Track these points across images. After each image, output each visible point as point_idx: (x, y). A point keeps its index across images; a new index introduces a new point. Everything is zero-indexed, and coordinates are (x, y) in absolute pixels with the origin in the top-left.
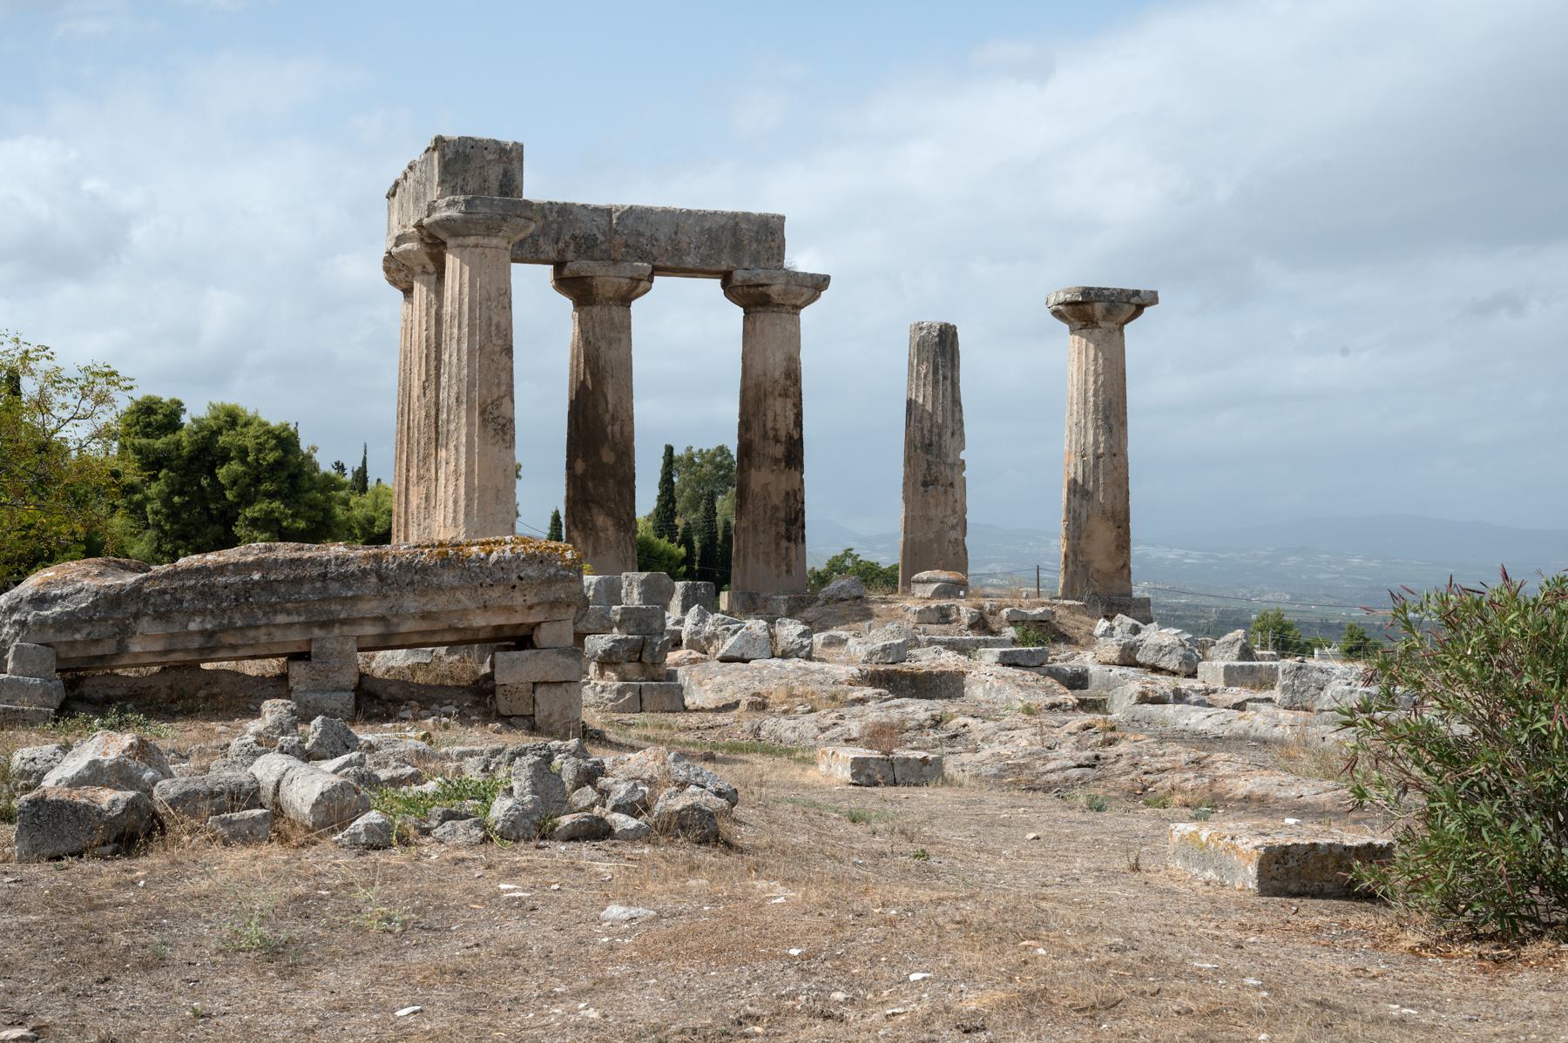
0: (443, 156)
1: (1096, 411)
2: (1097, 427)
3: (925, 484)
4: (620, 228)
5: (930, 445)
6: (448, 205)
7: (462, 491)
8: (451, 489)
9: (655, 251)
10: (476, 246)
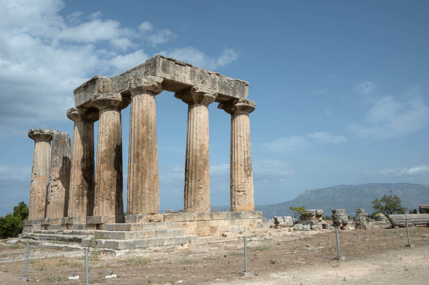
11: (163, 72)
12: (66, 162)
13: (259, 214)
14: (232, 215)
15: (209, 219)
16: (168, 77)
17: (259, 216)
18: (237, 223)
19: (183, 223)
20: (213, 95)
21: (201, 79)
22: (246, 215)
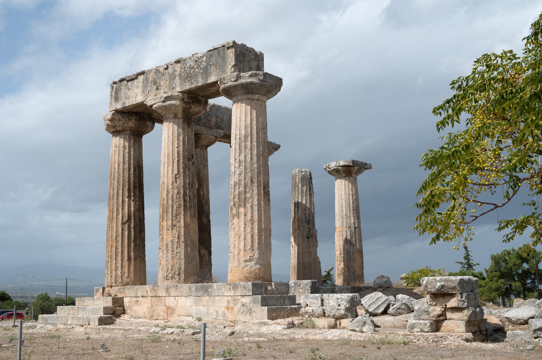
0: (236, 51)
1: (353, 210)
2: (354, 216)
3: (308, 238)
4: (210, 113)
5: (309, 221)
6: (251, 76)
7: (256, 231)
8: (249, 229)
9: (223, 125)
10: (258, 100)
11: (115, 102)
12: (298, 210)
13: (245, 287)
14: (197, 289)
15: (164, 295)
16: (119, 106)
17: (244, 291)
18: (205, 303)
19: (135, 299)
20: (163, 102)
21: (155, 83)
22: (220, 289)
